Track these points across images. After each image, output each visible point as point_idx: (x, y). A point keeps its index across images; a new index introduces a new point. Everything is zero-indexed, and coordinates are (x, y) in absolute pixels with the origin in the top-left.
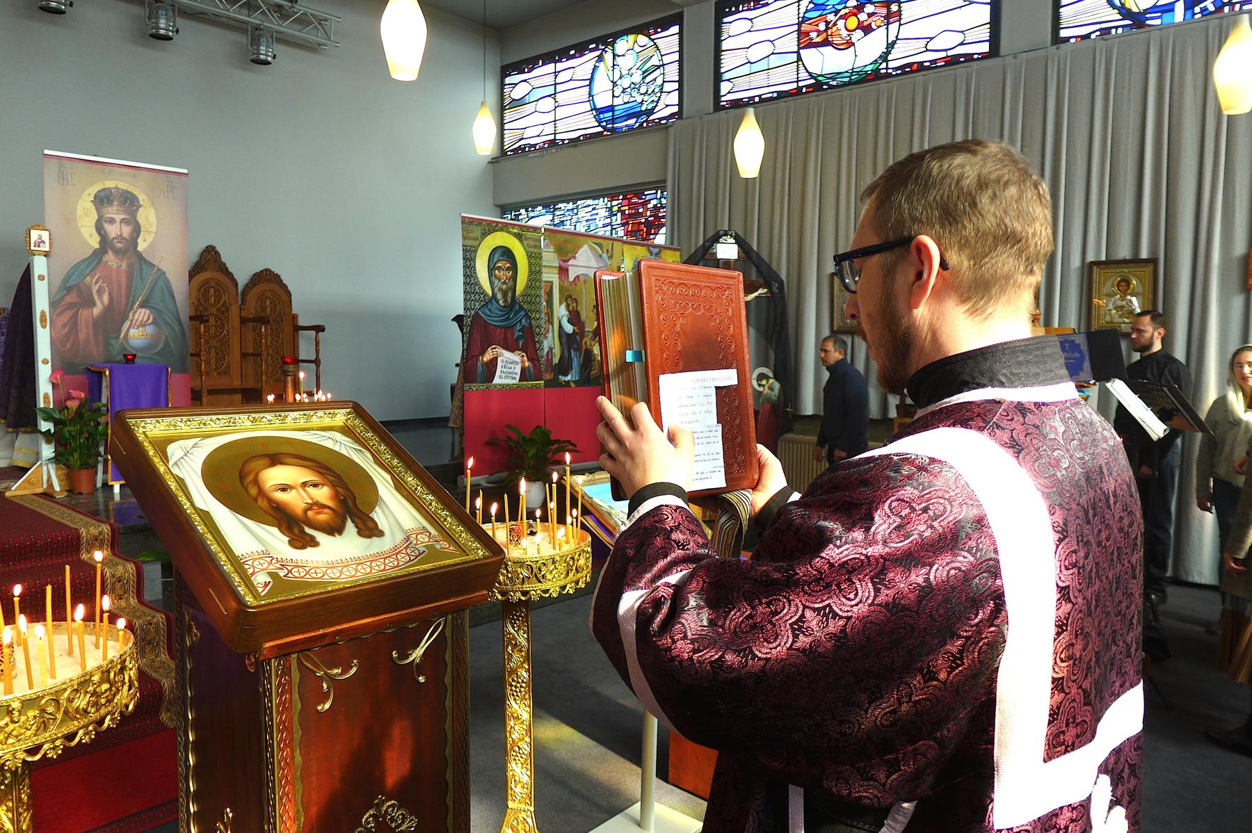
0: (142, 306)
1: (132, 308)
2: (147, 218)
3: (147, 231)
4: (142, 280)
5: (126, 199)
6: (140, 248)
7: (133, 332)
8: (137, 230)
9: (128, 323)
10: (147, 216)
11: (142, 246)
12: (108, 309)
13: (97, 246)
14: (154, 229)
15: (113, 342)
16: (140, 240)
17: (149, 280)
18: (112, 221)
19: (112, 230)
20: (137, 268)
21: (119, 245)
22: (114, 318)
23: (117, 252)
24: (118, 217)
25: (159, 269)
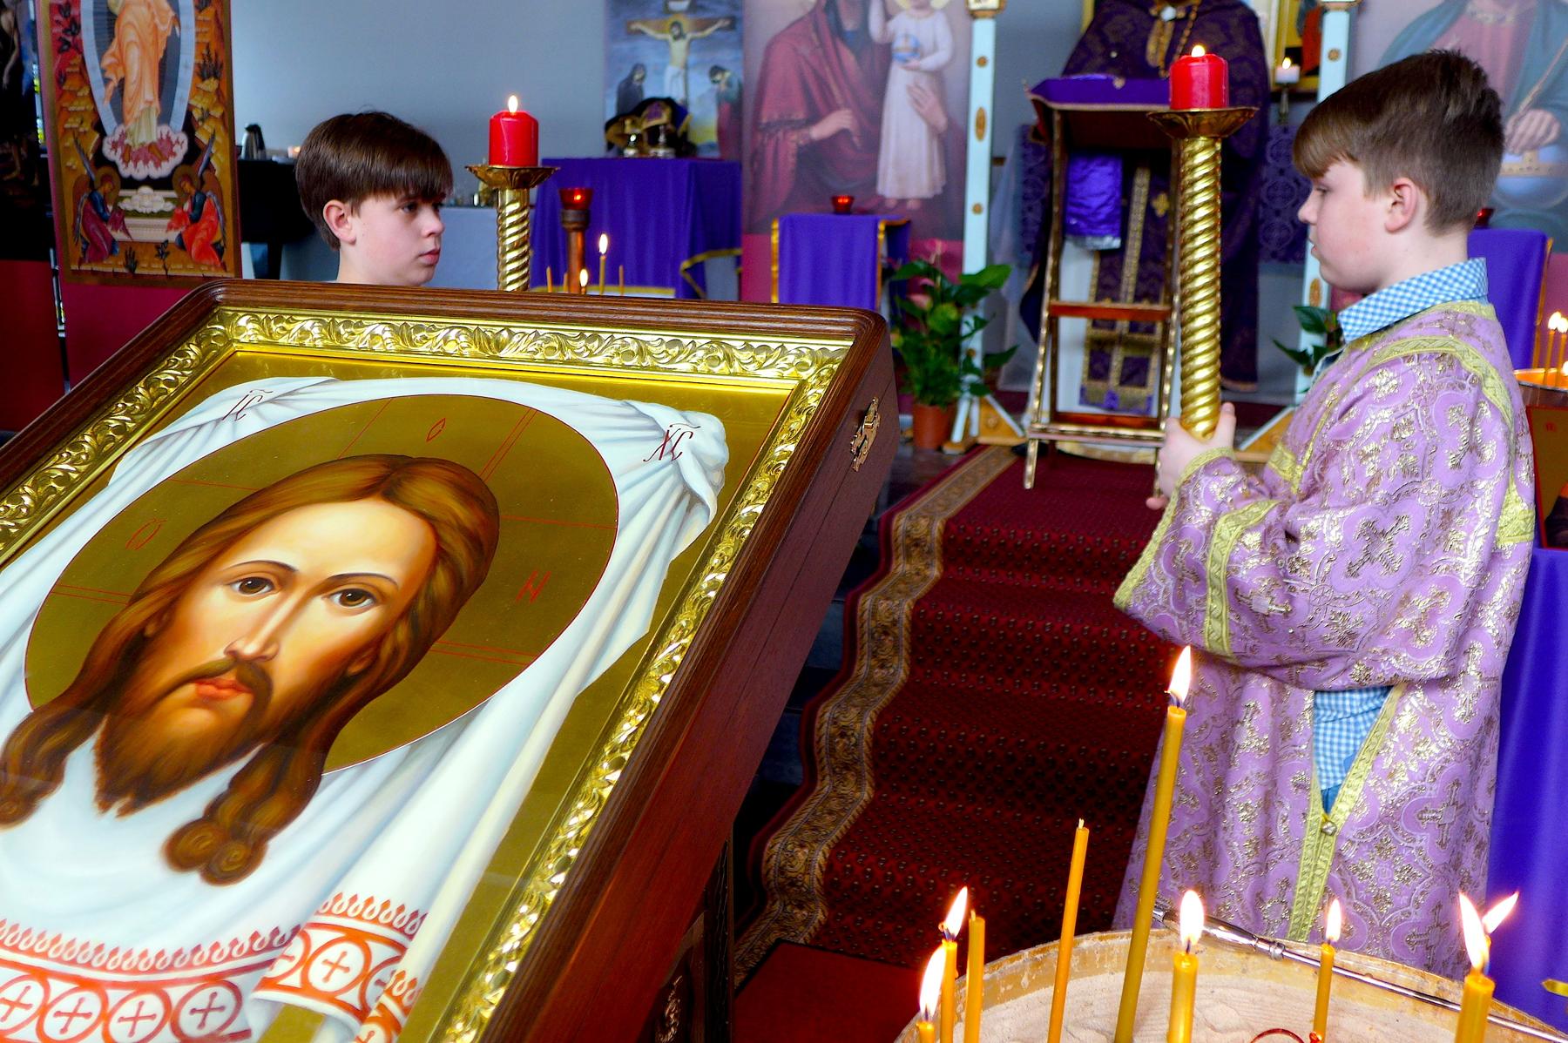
0: (1538, 104)
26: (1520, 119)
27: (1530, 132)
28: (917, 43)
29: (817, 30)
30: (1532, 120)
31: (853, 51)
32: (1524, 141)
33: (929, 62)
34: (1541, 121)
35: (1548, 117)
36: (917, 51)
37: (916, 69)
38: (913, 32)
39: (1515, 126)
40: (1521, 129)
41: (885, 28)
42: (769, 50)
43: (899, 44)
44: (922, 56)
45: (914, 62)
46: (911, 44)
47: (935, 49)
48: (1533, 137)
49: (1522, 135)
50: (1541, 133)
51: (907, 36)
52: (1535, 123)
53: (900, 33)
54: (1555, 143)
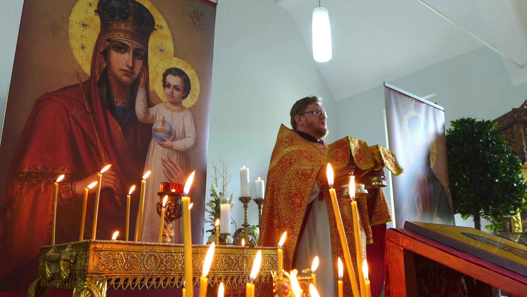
28: (171, 128)
29: (89, 99)
31: (120, 124)
33: (179, 144)
36: (171, 134)
37: (171, 148)
38: (168, 119)
41: (147, 112)
42: (40, 103)
43: (158, 125)
44: (174, 139)
45: (168, 142)
46: (167, 128)
47: (184, 136)
51: (164, 122)
53: (159, 118)
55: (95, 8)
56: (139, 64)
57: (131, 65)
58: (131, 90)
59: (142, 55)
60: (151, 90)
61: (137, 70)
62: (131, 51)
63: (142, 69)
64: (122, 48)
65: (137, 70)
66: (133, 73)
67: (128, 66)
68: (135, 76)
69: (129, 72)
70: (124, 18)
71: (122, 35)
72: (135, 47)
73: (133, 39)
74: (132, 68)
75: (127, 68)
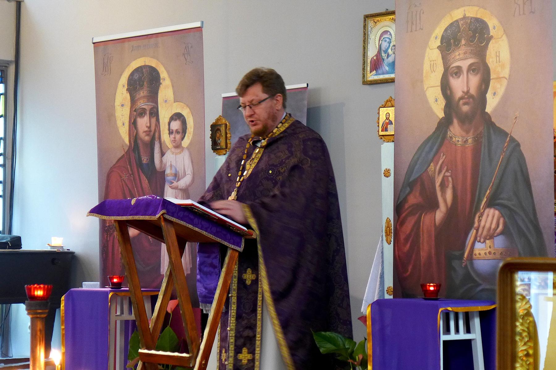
0: (491, 204)
1: (477, 209)
2: (498, 56)
3: (499, 78)
4: (491, 159)
5: (475, 32)
6: (489, 109)
7: (479, 246)
8: (485, 82)
9: (473, 232)
10: (500, 54)
11: (492, 103)
12: (452, 212)
13: (441, 115)
14: (506, 73)
15: (455, 264)
16: (489, 96)
17: (500, 158)
18: (458, 72)
19: (459, 86)
20: (484, 141)
21: (465, 108)
22: (459, 224)
23: (465, 120)
24: (465, 64)
25: (513, 140)
26: (482, 215)
27: (488, 225)
30: (488, 215)
32: (485, 233)
34: (493, 217)
35: (497, 212)
39: (480, 221)
40: (482, 224)
48: (490, 227)
49: (484, 228)
50: (493, 226)
52: (490, 219)
54: (502, 233)
55: (126, 87)
56: (154, 120)
57: (148, 125)
58: (151, 146)
59: (154, 113)
60: (162, 140)
61: (153, 128)
62: (148, 112)
63: (156, 125)
64: (142, 113)
65: (153, 128)
66: (150, 131)
67: (147, 127)
68: (152, 133)
69: (148, 133)
70: (142, 86)
71: (142, 101)
72: (150, 107)
73: (148, 101)
74: (149, 127)
75: (146, 129)
